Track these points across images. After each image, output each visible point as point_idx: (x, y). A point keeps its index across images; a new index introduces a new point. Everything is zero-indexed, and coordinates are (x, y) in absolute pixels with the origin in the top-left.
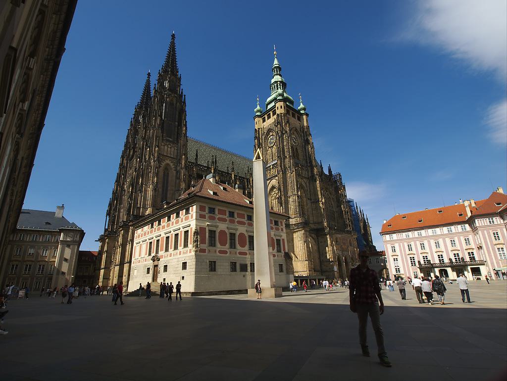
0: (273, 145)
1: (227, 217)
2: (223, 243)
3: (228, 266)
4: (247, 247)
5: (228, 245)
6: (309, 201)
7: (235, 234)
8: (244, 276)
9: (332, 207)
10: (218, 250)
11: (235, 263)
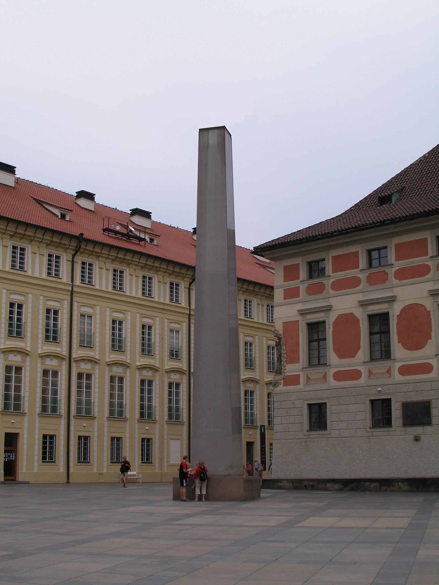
1: (360, 272)
3: (365, 415)
5: (363, 354)
7: (387, 314)
8: (417, 439)
10: (333, 371)
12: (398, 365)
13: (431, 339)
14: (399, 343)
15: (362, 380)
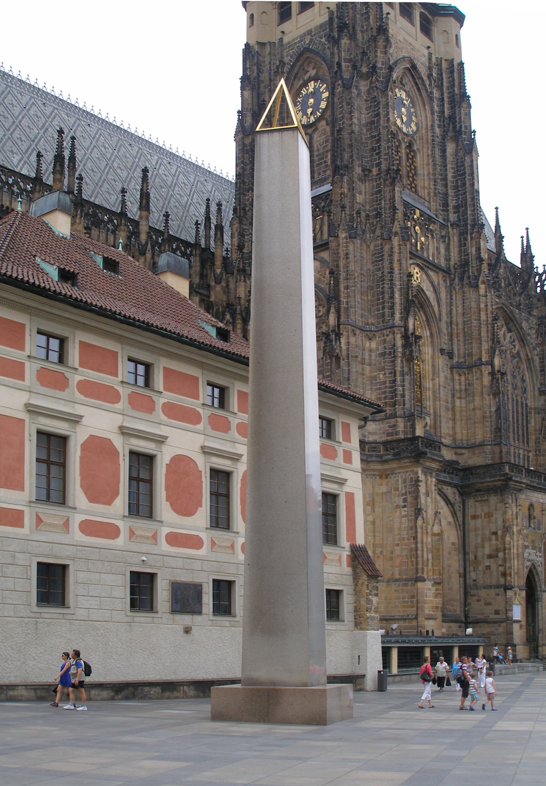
0: (318, 120)
2: (100, 494)
4: (203, 515)
6: (442, 362)
9: (525, 391)
11: (152, 577)
12: (165, 531)
13: (201, 506)
14: (167, 501)
15: (121, 541)
